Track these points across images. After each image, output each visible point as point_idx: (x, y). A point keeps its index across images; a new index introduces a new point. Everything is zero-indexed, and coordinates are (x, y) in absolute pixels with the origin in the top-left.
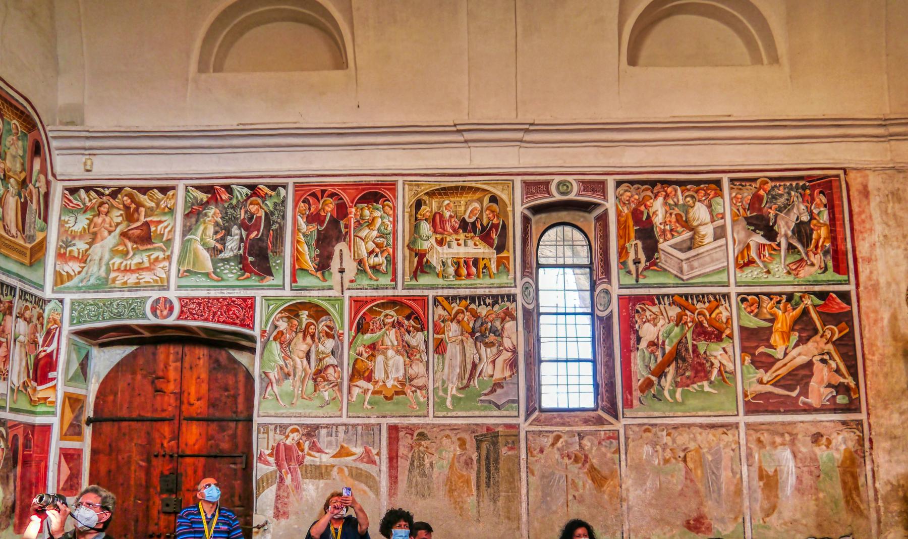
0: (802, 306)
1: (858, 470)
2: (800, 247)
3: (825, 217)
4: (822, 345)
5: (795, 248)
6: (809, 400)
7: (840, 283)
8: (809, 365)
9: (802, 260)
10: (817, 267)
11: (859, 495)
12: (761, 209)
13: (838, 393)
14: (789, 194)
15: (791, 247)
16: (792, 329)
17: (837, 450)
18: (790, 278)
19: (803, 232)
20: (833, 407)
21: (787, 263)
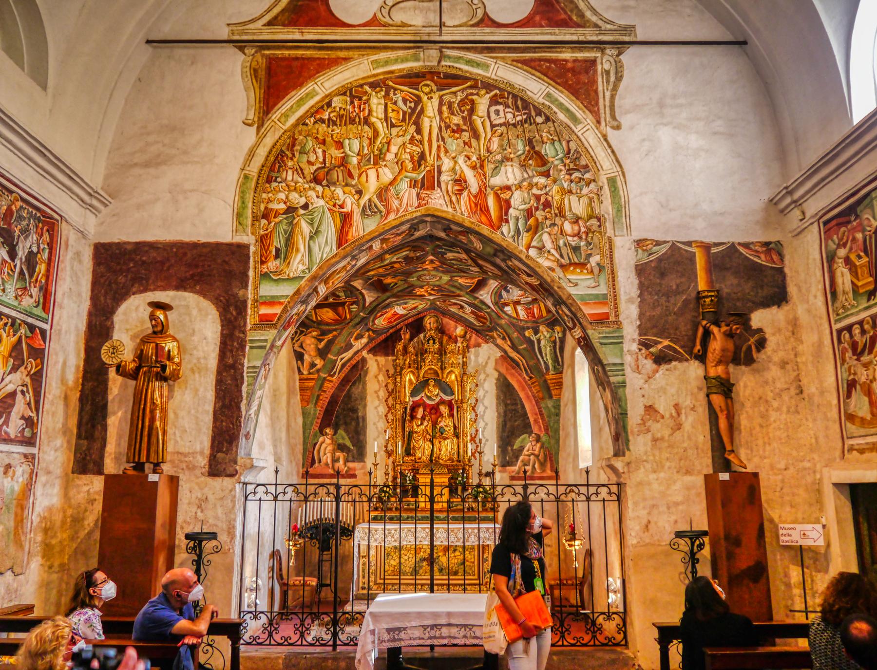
0: (19, 334)
1: (25, 503)
2: (27, 274)
3: (46, 255)
4: (24, 376)
5: (24, 275)
6: (8, 430)
7: (38, 318)
8: (13, 395)
9: (25, 288)
10: (33, 300)
11: (22, 528)
12: (10, 224)
13: (27, 427)
14: (30, 220)
15: (21, 273)
16: (10, 356)
17: (17, 482)
18: (16, 303)
19: (31, 260)
20: (21, 439)
21: (18, 286)
